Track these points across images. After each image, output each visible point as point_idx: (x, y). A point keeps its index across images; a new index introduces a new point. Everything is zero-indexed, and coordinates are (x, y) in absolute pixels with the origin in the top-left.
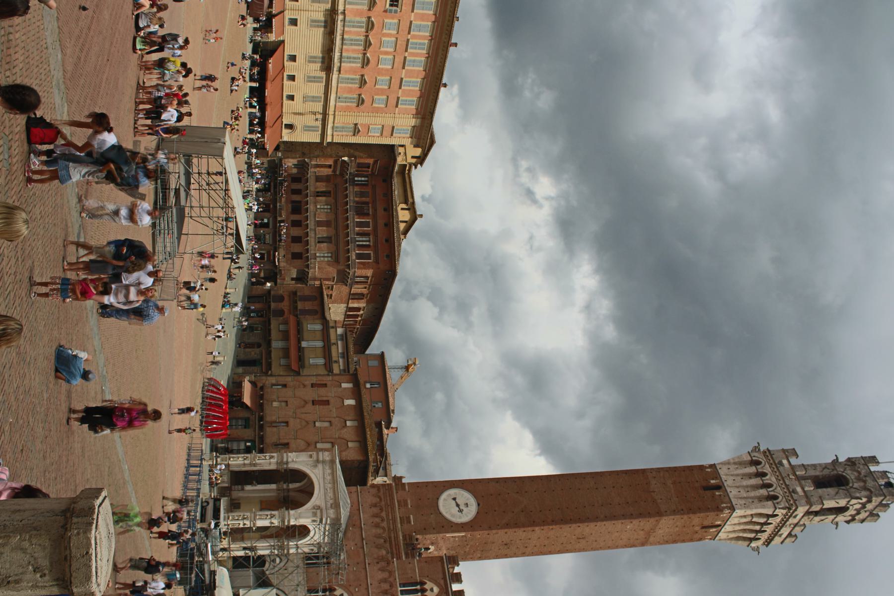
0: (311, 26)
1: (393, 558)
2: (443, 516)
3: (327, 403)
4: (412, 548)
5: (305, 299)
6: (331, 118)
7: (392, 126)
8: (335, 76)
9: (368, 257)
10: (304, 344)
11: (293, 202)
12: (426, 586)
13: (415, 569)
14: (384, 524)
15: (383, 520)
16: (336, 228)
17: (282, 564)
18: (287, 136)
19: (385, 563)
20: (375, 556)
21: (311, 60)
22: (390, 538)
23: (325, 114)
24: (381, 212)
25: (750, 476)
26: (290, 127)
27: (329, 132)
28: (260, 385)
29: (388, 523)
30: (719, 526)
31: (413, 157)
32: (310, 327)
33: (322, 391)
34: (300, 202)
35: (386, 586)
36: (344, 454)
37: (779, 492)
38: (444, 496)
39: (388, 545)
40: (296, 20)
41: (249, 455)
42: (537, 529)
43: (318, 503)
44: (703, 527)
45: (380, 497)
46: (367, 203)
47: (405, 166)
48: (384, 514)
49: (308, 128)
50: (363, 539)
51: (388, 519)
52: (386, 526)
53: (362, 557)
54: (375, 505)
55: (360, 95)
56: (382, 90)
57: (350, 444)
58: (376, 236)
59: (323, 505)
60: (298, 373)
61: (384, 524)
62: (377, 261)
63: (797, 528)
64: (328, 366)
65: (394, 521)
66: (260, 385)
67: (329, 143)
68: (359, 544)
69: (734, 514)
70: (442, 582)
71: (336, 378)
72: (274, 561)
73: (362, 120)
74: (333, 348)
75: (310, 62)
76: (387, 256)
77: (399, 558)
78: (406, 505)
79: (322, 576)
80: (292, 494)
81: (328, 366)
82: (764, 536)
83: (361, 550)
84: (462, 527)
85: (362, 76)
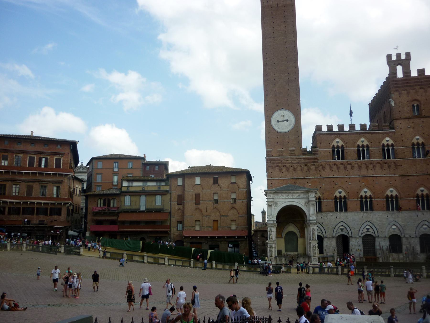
1: (317, 162)
2: (290, 130)
3: (198, 196)
9: (58, 161)
10: (143, 208)
12: (336, 145)
14: (295, 165)
16: (34, 181)
20: (315, 172)
22: (304, 163)
29: (294, 163)
34: (9, 208)
35: (335, 167)
36: (241, 186)
38: (276, 128)
39: (308, 164)
41: (269, 245)
43: (303, 203)
50: (304, 178)
52: (296, 165)
53: (315, 180)
54: (280, 170)
57: (233, 181)
59: (306, 200)
60: (170, 213)
62: (62, 154)
64: (163, 193)
68: (307, 181)
70: (333, 136)
71: (172, 188)
77: (317, 159)
78: (281, 152)
79: (328, 203)
81: (163, 193)
83: (311, 180)
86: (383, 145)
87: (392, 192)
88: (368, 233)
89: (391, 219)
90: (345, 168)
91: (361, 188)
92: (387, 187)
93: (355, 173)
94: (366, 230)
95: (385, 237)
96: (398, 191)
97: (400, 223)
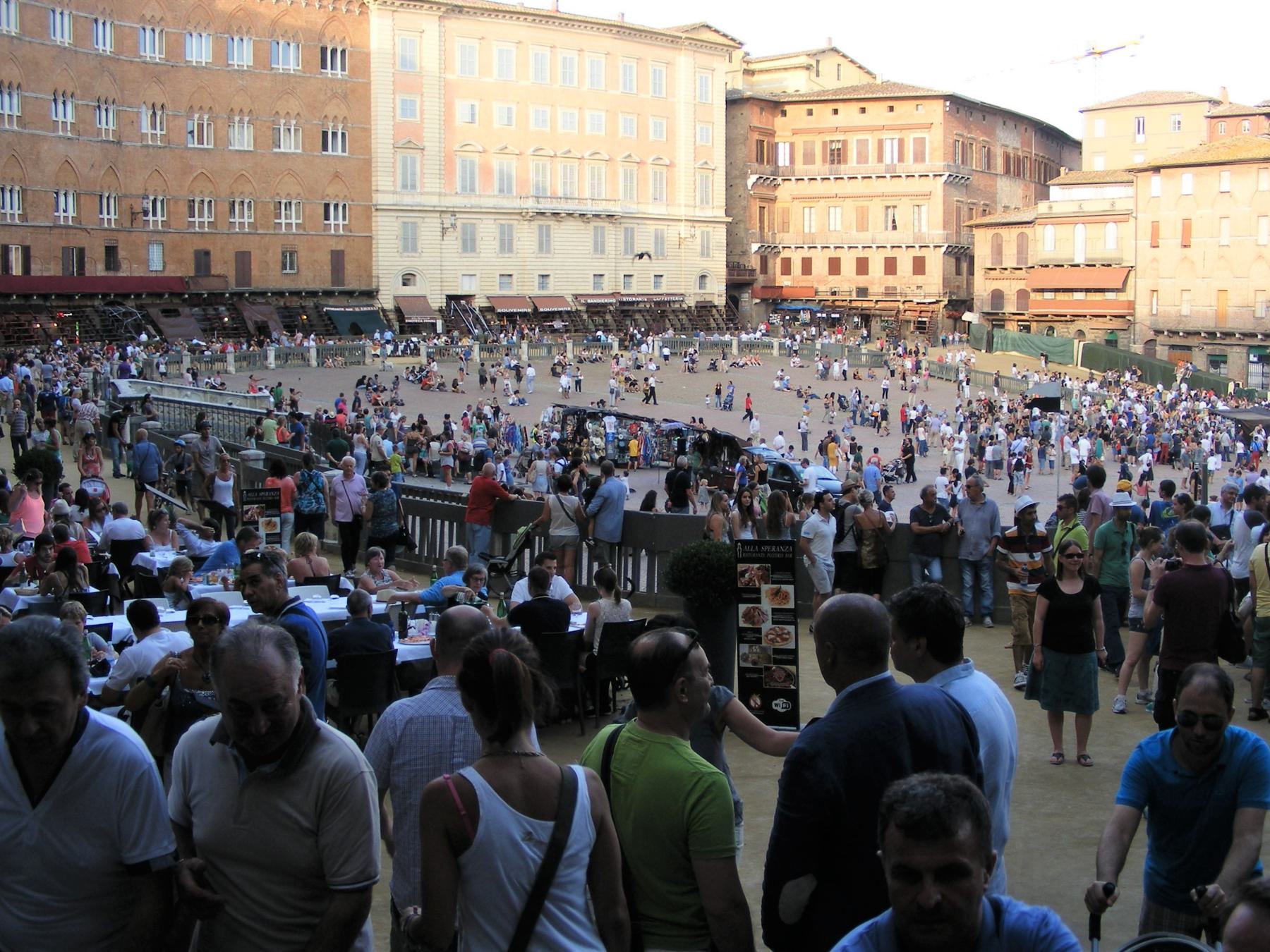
0: (548, 251)
3: (1187, 226)
5: (998, 251)
9: (920, 142)
10: (1079, 260)
21: (599, 248)
27: (708, 213)
28: (1151, 335)
32: (1049, 245)
33: (1163, 232)
64: (1121, 217)
66: (1151, 335)
67: (727, 215)
74: (1089, 208)
75: (603, 251)
81: (1121, 217)
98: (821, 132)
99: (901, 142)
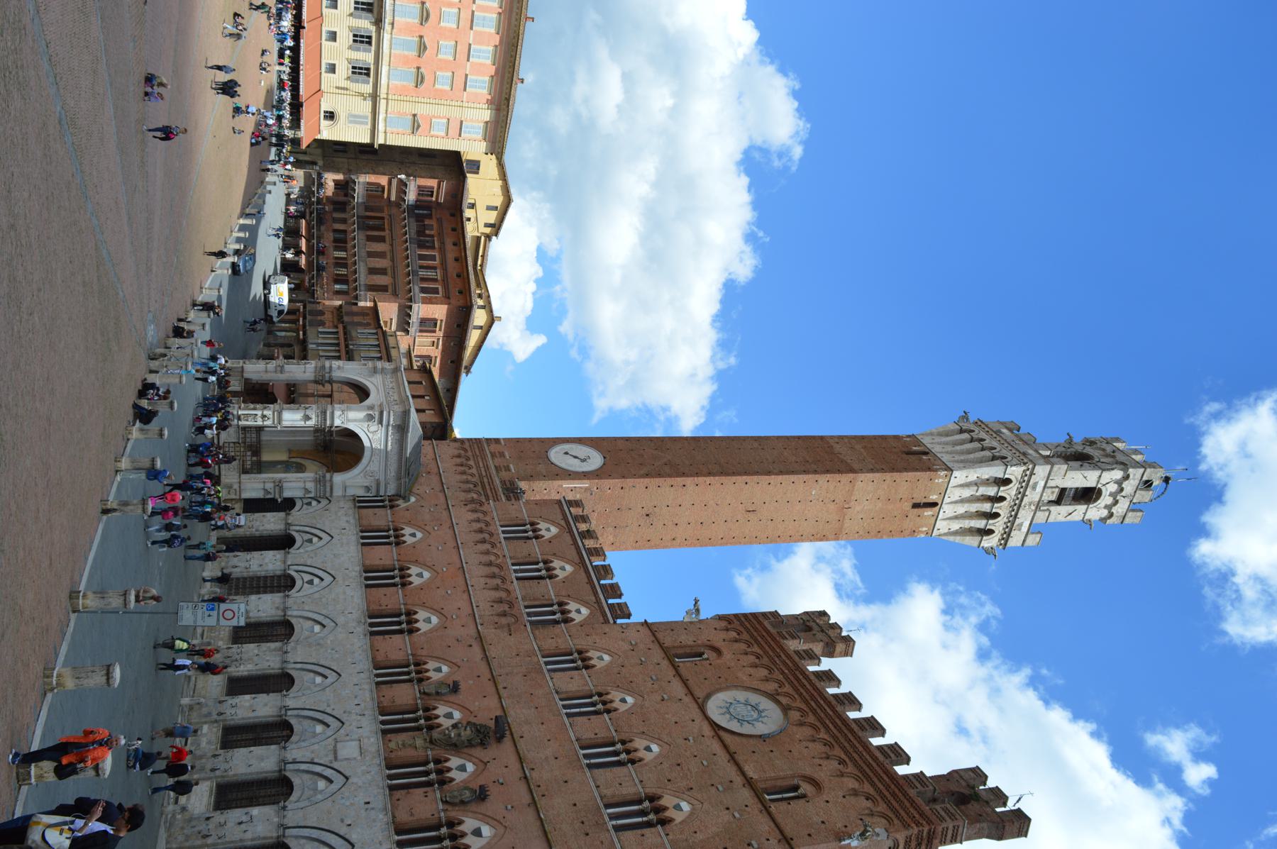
1: (488, 499)
4: (512, 492)
6: (383, 103)
7: (456, 124)
8: (386, 37)
9: (436, 291)
11: (335, 231)
13: (520, 510)
15: (468, 459)
16: (392, 260)
17: (321, 505)
18: (328, 132)
19: (475, 505)
22: (482, 483)
23: (374, 97)
24: (449, 242)
25: (962, 442)
26: (330, 116)
27: (381, 126)
30: (934, 504)
31: (487, 225)
34: (344, 232)
35: (478, 525)
37: (1004, 453)
40: (335, 33)
42: (689, 481)
44: (916, 506)
45: (466, 450)
46: (432, 236)
47: (478, 239)
48: (471, 463)
49: (355, 119)
51: (478, 467)
54: (459, 456)
55: (418, 68)
56: (446, 61)
58: (445, 269)
61: (474, 471)
63: (1039, 514)
65: (487, 468)
68: (438, 488)
69: (953, 482)
70: (563, 523)
72: (309, 504)
73: (421, 110)
76: (460, 292)
77: (496, 499)
79: (381, 518)
80: (335, 437)
82: (998, 525)
84: (585, 475)
85: (421, 37)
86: (561, 604)
87: (426, 621)
88: (299, 583)
89: (341, 620)
90: (483, 541)
91: (429, 567)
92: (439, 612)
93: (472, 557)
94: (307, 577)
95: (285, 609)
96: (431, 631)
97: (331, 637)
98: (441, 235)
99: (435, 280)
